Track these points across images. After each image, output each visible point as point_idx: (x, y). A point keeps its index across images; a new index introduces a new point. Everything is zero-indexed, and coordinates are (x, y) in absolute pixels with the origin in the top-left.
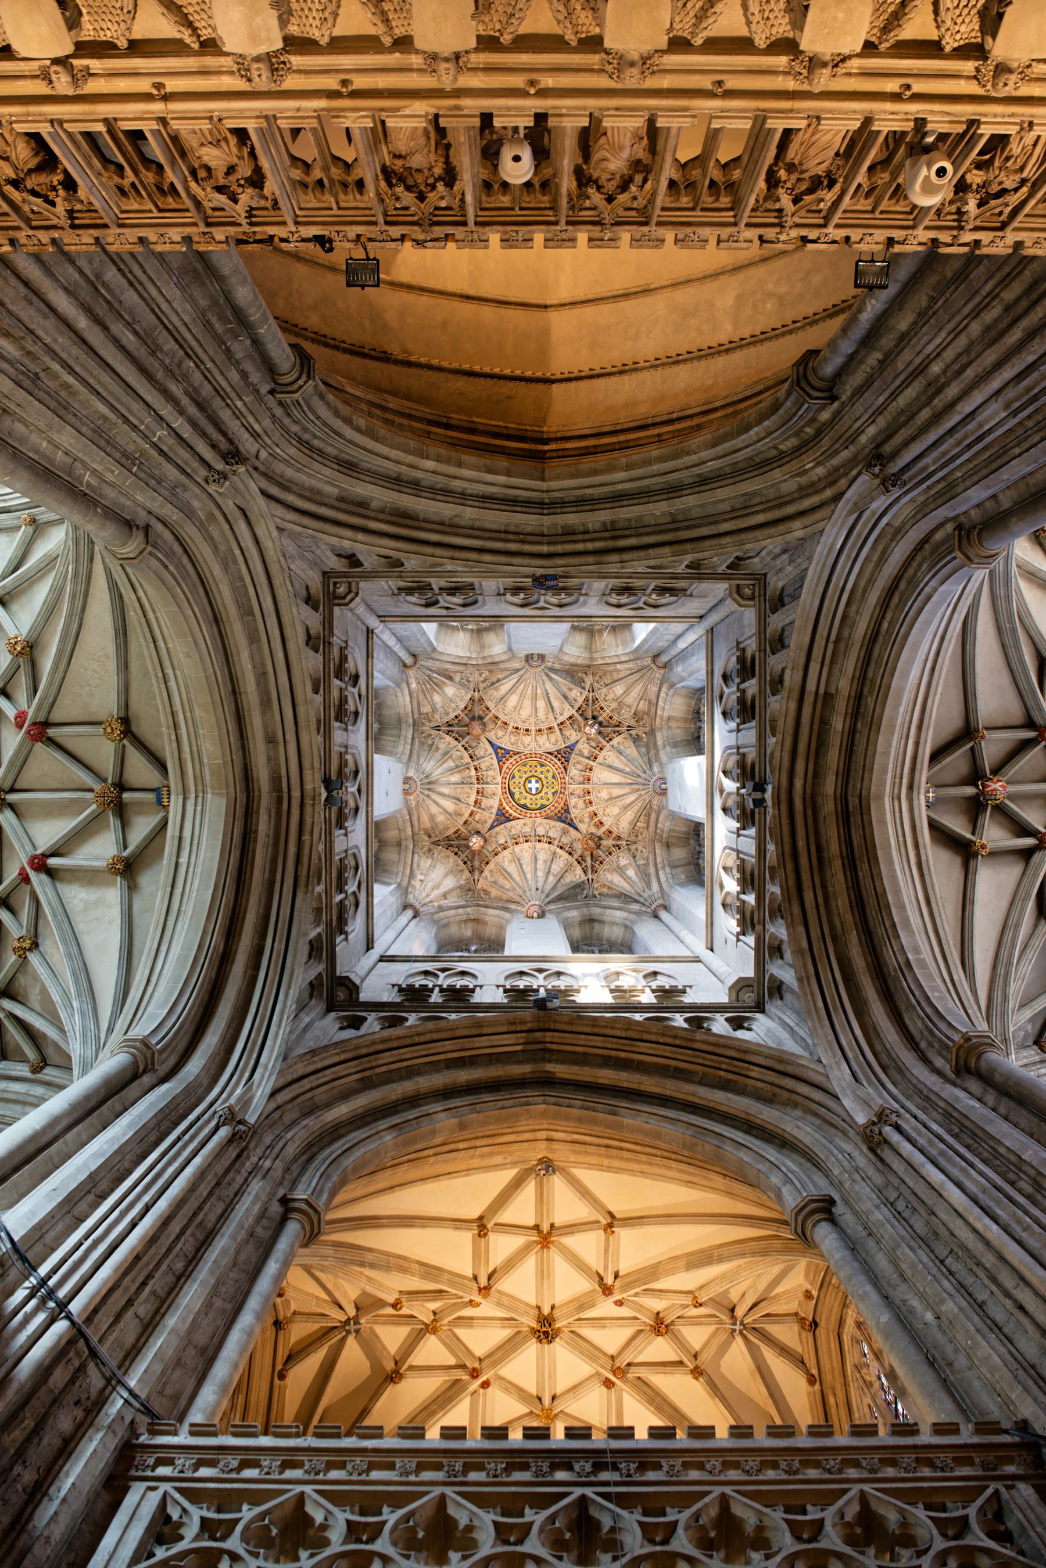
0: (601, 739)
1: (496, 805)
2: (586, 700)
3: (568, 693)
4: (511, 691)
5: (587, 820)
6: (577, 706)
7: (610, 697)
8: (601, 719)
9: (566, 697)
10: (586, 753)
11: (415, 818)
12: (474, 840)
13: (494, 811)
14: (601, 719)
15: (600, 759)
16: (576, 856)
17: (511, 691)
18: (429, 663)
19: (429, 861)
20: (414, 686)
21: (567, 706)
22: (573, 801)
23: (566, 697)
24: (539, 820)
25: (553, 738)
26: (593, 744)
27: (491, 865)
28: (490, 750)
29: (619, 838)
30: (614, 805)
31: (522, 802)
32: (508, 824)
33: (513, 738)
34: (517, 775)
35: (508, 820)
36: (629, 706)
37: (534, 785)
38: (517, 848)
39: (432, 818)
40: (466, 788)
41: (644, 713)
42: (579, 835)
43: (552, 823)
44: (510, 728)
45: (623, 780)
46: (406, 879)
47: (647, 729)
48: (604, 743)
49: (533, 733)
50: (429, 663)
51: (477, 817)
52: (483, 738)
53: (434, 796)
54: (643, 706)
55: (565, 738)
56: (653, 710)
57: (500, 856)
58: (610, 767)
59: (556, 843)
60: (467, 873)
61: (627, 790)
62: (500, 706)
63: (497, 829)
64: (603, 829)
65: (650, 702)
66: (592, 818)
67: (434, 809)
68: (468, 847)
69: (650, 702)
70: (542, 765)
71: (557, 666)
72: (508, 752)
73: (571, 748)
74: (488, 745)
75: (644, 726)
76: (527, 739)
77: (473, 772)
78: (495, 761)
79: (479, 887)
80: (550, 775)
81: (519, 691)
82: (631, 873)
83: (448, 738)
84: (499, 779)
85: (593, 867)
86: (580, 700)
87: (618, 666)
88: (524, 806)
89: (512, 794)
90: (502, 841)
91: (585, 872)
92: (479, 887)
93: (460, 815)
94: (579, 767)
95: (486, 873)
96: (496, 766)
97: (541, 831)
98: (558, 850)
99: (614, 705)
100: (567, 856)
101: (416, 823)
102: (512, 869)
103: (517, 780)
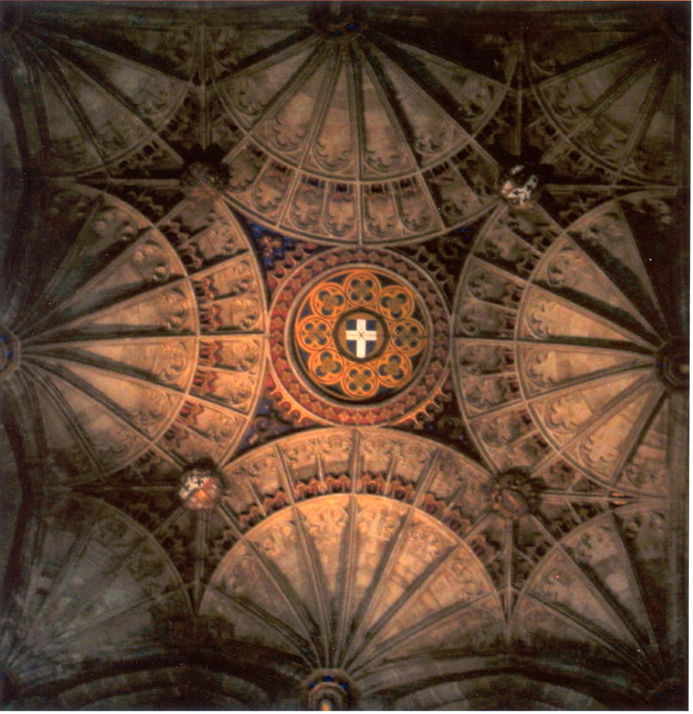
0: (546, 217)
1: (256, 389)
2: (507, 106)
6: (480, 122)
7: (573, 100)
12: (192, 484)
13: (251, 405)
21: (451, 125)
22: (468, 382)
25: (414, 210)
34: (317, 303)
35: (290, 429)
40: (171, 344)
48: (555, 226)
49: (357, 194)
52: (221, 206)
60: (171, 574)
63: (257, 454)
66: (517, 432)
70: (386, 282)
73: (469, 233)
74: (236, 229)
76: (344, 212)
77: (190, 302)
78: (255, 270)
80: (407, 310)
84: (265, 320)
85: (517, 563)
86: (490, 108)
90: (270, 486)
91: (495, 575)
93: (156, 416)
96: (258, 283)
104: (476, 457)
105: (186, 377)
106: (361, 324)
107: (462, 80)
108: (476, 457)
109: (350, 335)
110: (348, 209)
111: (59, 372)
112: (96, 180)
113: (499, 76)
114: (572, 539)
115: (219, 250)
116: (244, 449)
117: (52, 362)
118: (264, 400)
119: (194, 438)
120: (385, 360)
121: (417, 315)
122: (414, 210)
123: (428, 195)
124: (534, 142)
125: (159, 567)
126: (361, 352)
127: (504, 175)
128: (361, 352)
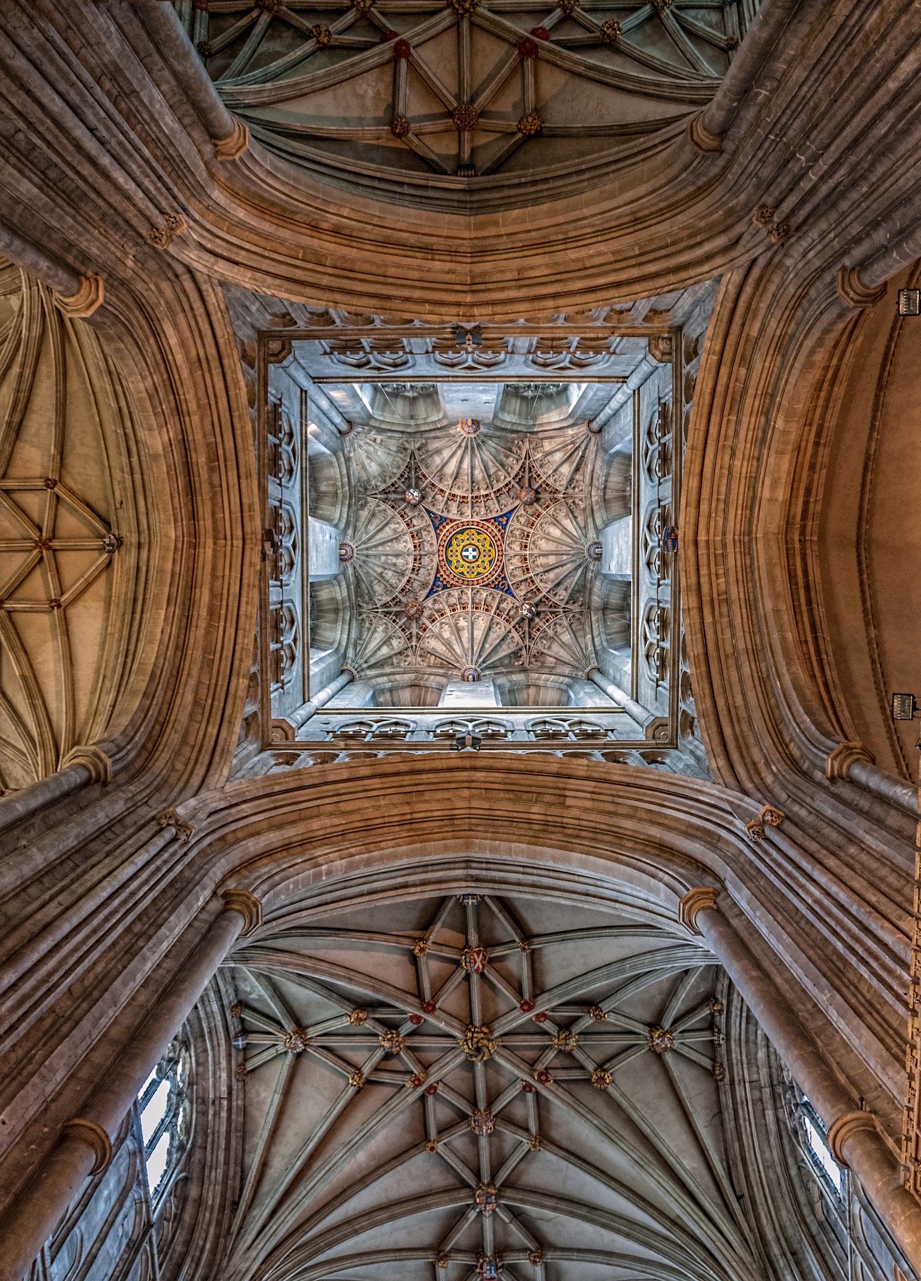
0: (516, 620)
1: (450, 516)
3: (563, 587)
4: (565, 531)
5: (437, 607)
6: (550, 596)
7: (559, 629)
8: (537, 620)
9: (558, 585)
10: (503, 605)
11: (438, 434)
12: (416, 494)
13: (445, 514)
14: (537, 620)
15: (497, 619)
16: (400, 596)
17: (565, 531)
18: (592, 448)
19: (394, 449)
20: (570, 432)
21: (550, 586)
22: (456, 593)
23: (558, 585)
24: (436, 559)
26: (512, 613)
27: (390, 512)
28: (506, 510)
29: (419, 638)
30: (452, 633)
31: (454, 542)
32: (432, 528)
33: (517, 533)
36: (549, 648)
37: (471, 554)
38: (408, 537)
39: (438, 451)
41: (543, 663)
42: (421, 599)
43: (433, 572)
44: (527, 529)
45: (476, 642)
46: (377, 424)
47: (526, 665)
48: (513, 623)
49: (523, 552)
50: (592, 448)
51: (439, 497)
52: (518, 502)
53: (460, 453)
54: (550, 661)
55: (518, 585)
56: (546, 670)
57: (400, 520)
58: (490, 629)
59: (413, 576)
60: (383, 487)
61: (467, 645)
62: (550, 519)
64: (427, 623)
65: (553, 668)
67: (446, 454)
68: (409, 487)
69: (553, 668)
70: (490, 562)
71: (590, 575)
72: (504, 527)
74: (510, 508)
75: (530, 663)
76: (516, 547)
77: (483, 492)
78: (495, 515)
79: (369, 499)
80: (481, 570)
81: (565, 538)
82: (385, 650)
83: (517, 468)
85: (390, 613)
87: (589, 636)
88: (450, 544)
89: (462, 532)
90: (415, 522)
92: (369, 499)
94: (490, 598)
95: (383, 506)
97: (425, 561)
98: (406, 578)
99: (551, 632)
100: (401, 586)
101: (432, 434)
102: (388, 532)
103: (476, 537)
104: (427, 597)
105: (456, 491)
106: (475, 553)
107: (566, 590)
108: (427, 597)
109: (470, 550)
110: (518, 549)
111: (460, 446)
112: (528, 456)
113: (567, 603)
114: (400, 633)
115: (503, 502)
116: (428, 512)
117: (463, 444)
118: (446, 519)
119: (432, 494)
120: (462, 562)
121: (479, 574)
122: (515, 572)
123: (523, 578)
124: (542, 615)
125: (385, 481)
126: (464, 554)
127: (530, 604)
128: (464, 554)
